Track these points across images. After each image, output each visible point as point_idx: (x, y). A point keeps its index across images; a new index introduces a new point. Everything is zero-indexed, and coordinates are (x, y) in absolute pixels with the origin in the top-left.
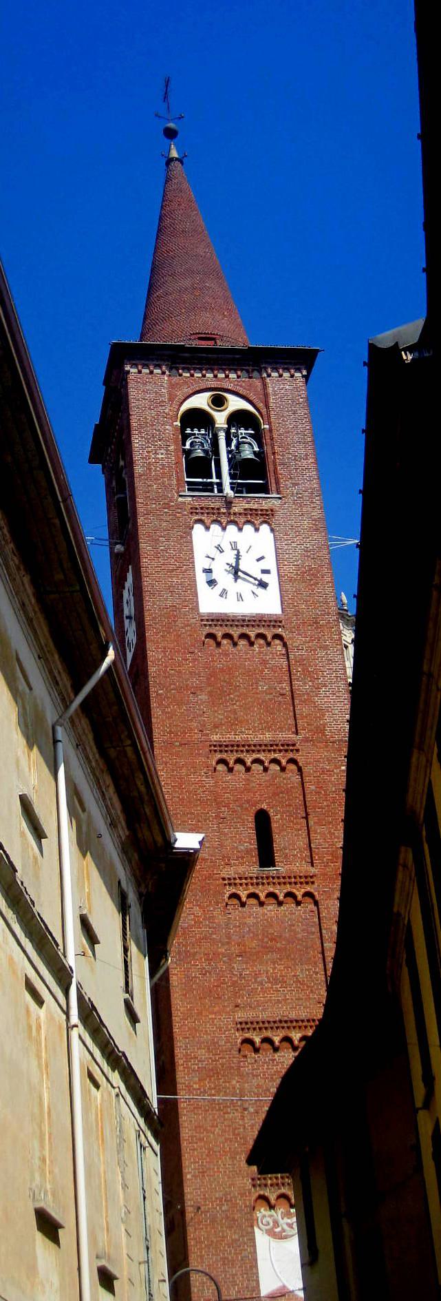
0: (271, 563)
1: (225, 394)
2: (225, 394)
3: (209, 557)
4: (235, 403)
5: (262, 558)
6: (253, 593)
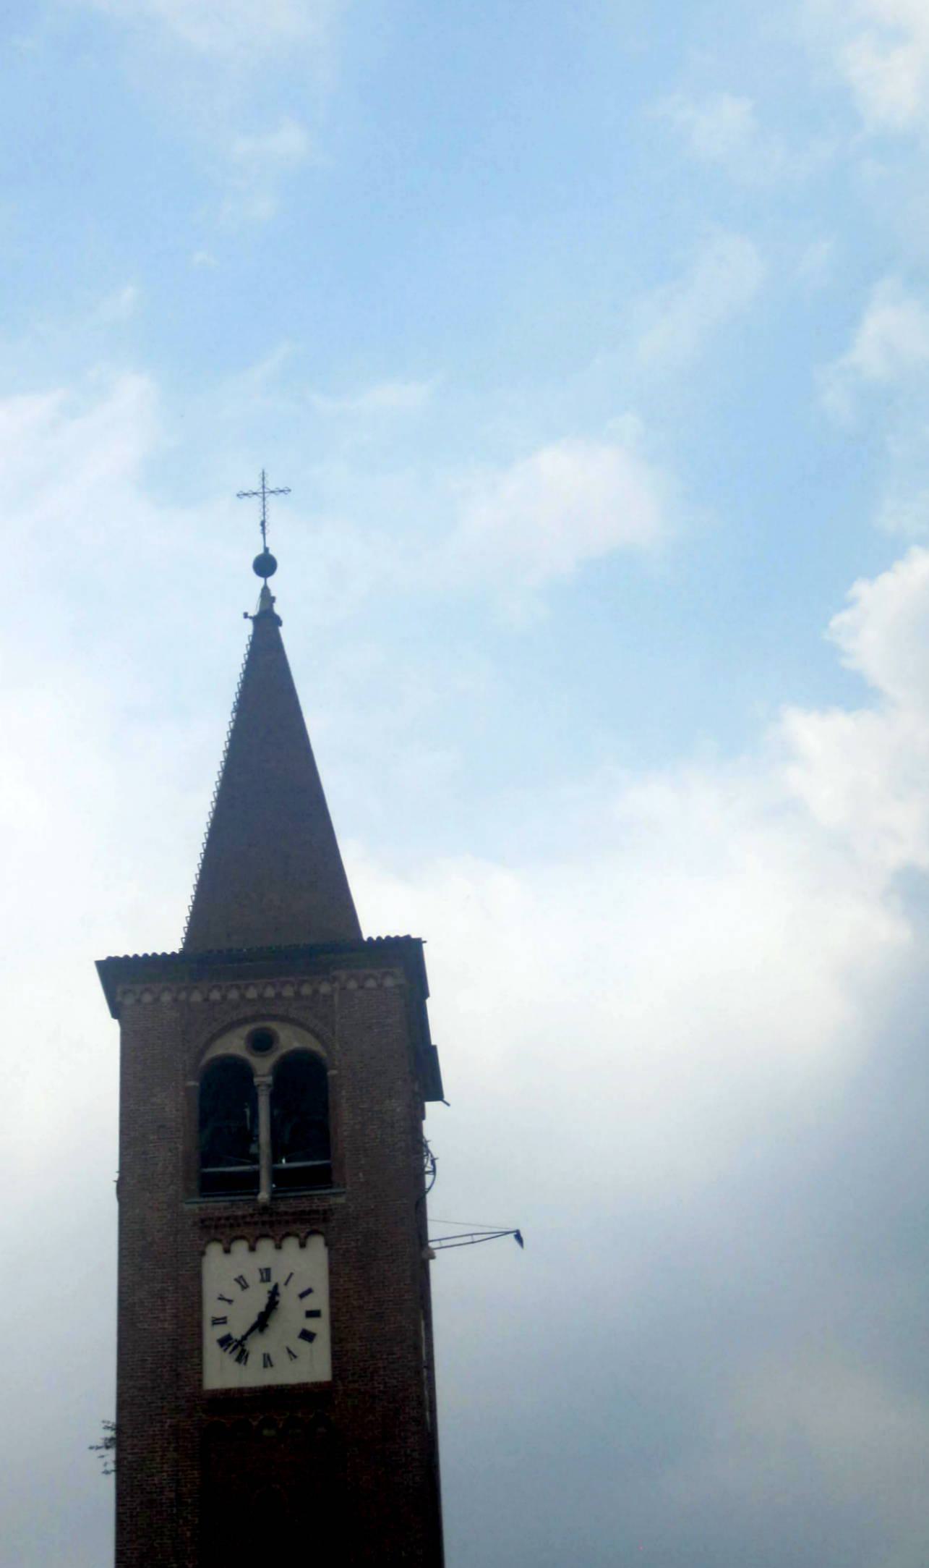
0: (320, 1300)
1: (273, 1025)
2: (273, 1025)
4: (290, 1040)
5: (309, 1291)
6: (290, 1352)
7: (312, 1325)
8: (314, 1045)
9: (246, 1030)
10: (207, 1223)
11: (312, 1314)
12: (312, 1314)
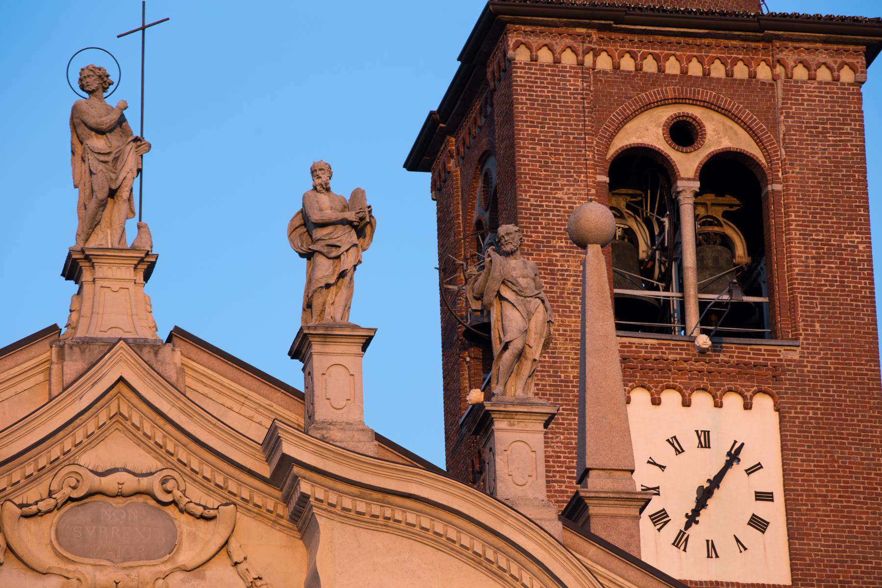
3: (655, 464)
5: (758, 467)
6: (738, 541)
7: (763, 510)
8: (745, 143)
9: (666, 113)
10: (634, 363)
11: (763, 496)
12: (763, 496)
